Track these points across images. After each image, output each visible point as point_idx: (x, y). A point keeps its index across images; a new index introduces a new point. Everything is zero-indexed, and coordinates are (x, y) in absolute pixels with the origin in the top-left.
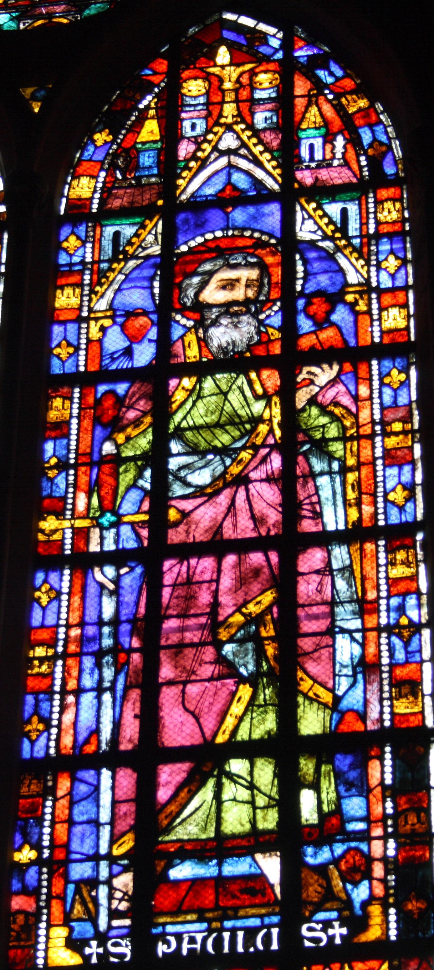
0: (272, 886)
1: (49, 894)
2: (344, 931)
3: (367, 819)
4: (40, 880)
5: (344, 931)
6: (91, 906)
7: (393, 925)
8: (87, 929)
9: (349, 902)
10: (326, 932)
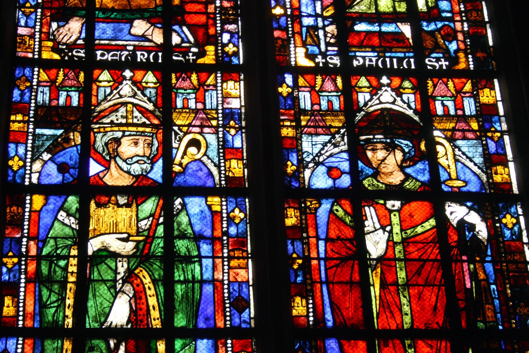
0: (408, 39)
1: (293, 31)
2: (447, 63)
3: (451, 11)
4: (287, 24)
5: (447, 63)
6: (315, 39)
7: (471, 63)
8: (316, 49)
9: (447, 50)
10: (438, 63)
